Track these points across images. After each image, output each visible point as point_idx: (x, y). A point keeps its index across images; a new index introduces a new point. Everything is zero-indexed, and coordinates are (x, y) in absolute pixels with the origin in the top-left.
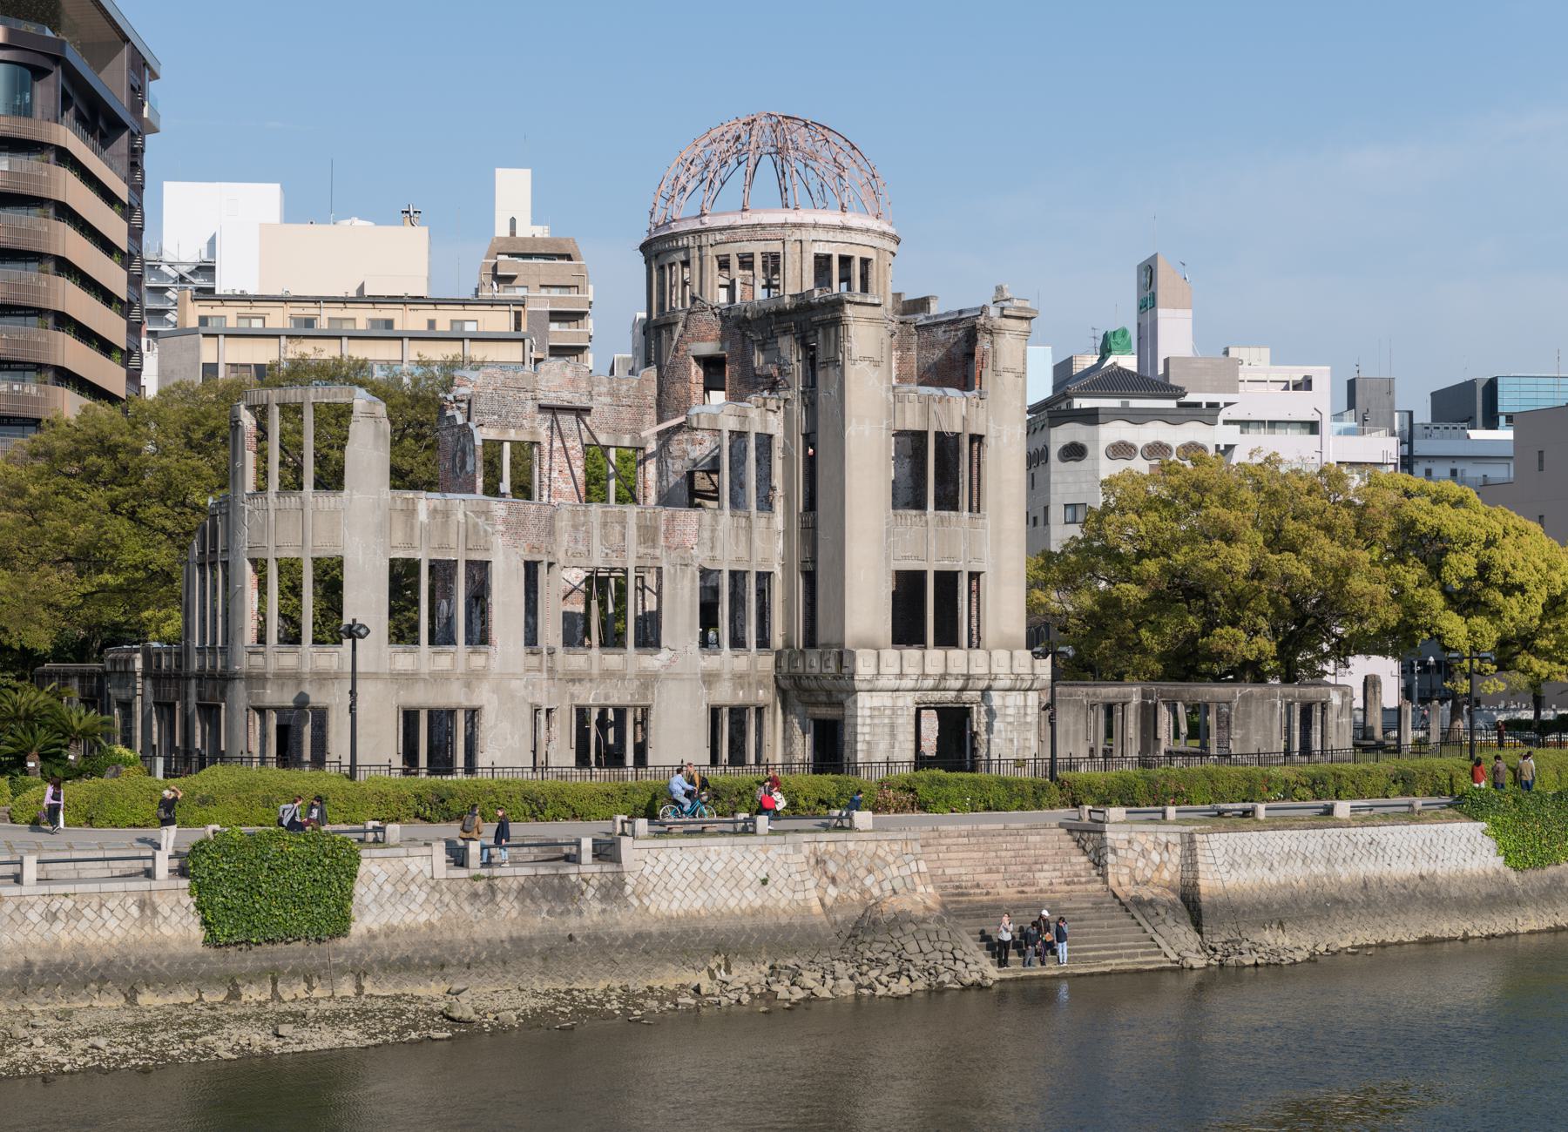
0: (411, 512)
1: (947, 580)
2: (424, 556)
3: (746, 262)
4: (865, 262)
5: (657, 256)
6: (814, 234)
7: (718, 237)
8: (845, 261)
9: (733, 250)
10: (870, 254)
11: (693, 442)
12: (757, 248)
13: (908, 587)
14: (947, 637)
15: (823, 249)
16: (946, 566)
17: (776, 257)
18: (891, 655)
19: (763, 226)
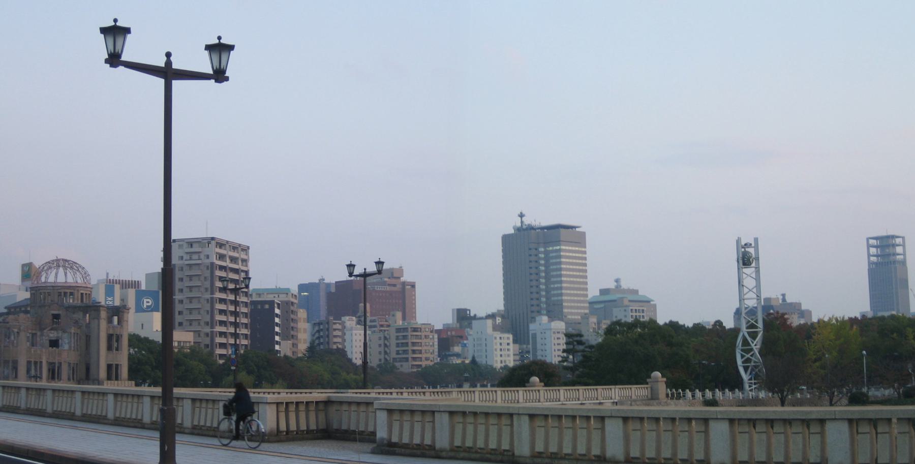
0: (31, 351)
1: (117, 366)
2: (33, 360)
3: (65, 293)
4: (89, 294)
5: (39, 290)
6: (81, 289)
7: (59, 288)
8: (86, 294)
9: (62, 291)
10: (90, 293)
11: (51, 333)
12: (68, 291)
13: (109, 367)
14: (117, 379)
15: (82, 292)
16: (117, 363)
17: (72, 292)
18: (109, 382)
19: (70, 286)
